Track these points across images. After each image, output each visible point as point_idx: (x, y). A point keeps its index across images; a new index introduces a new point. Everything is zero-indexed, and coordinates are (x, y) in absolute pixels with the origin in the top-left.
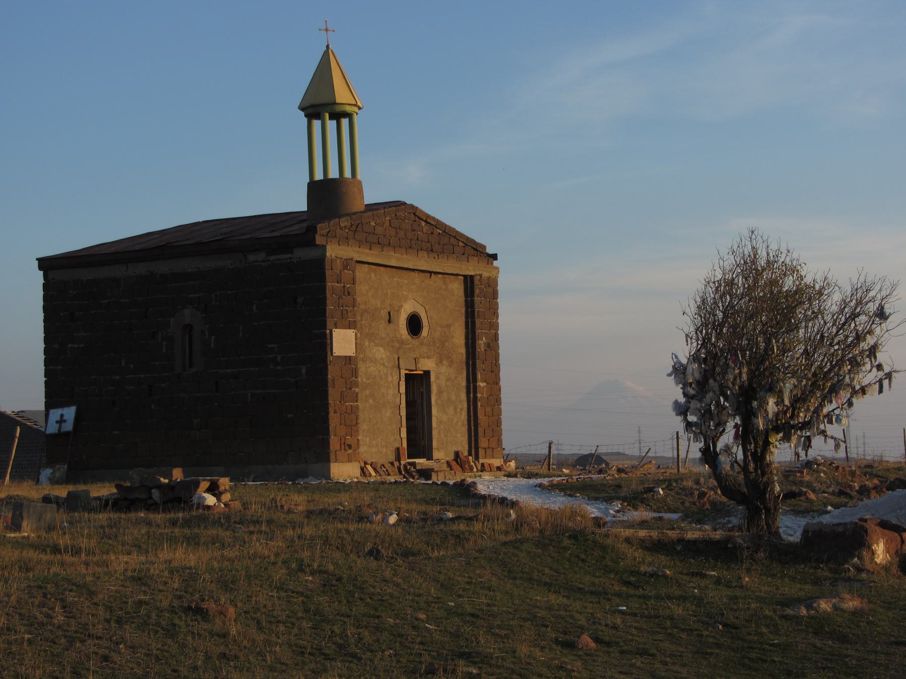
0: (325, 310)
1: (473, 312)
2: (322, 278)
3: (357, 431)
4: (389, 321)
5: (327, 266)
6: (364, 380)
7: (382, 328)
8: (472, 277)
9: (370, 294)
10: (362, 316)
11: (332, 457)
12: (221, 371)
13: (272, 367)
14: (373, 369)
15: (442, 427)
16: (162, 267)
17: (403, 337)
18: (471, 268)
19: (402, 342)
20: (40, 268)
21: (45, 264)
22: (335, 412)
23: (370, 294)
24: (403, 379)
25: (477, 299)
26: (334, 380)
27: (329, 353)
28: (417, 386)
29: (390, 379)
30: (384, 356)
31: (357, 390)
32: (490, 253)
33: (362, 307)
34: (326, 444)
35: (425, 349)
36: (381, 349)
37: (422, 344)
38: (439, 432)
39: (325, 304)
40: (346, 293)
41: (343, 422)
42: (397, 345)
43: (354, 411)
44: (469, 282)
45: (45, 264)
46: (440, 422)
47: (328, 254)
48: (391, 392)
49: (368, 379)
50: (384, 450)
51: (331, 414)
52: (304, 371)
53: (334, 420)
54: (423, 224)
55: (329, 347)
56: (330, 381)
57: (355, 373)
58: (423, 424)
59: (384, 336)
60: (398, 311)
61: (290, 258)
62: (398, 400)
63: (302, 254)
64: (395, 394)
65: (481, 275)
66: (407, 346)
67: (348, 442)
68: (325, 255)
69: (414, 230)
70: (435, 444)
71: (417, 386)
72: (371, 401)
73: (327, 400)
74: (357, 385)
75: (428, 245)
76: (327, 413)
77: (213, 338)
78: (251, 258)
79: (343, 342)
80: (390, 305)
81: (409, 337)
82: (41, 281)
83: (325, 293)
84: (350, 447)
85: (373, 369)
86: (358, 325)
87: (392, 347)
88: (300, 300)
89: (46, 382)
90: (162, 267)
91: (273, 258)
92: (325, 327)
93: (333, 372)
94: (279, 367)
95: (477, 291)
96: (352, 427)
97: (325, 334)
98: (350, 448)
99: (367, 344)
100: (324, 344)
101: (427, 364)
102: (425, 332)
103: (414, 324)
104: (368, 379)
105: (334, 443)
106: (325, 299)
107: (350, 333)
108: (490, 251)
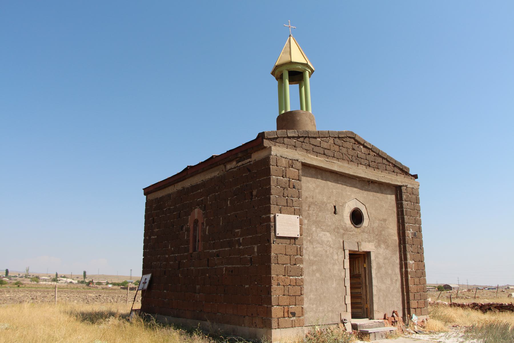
0: (269, 199)
1: (402, 211)
2: (267, 172)
3: (302, 300)
4: (335, 213)
5: (272, 162)
6: (312, 258)
7: (329, 218)
8: (400, 187)
9: (317, 191)
10: (309, 207)
11: (274, 324)
12: (211, 251)
13: (237, 247)
14: (319, 249)
15: (381, 293)
16: (187, 183)
17: (347, 226)
18: (398, 180)
19: (346, 230)
20: (145, 194)
21: (144, 189)
22: (278, 284)
23: (317, 191)
24: (347, 257)
25: (404, 203)
26: (277, 257)
27: (272, 234)
28: (359, 261)
29: (336, 257)
30: (330, 239)
31: (301, 266)
32: (412, 174)
33: (310, 200)
34: (269, 312)
35: (366, 236)
36: (328, 234)
37: (363, 232)
38: (379, 298)
39: (270, 193)
40: (291, 186)
41: (286, 293)
42: (342, 231)
43: (299, 285)
44: (398, 190)
45: (144, 189)
46: (380, 290)
47: (273, 153)
48: (336, 267)
49: (315, 257)
50: (330, 314)
51: (274, 286)
52: (256, 250)
53: (277, 292)
54: (362, 147)
55: (272, 229)
56: (273, 259)
57: (299, 252)
58: (366, 292)
59: (330, 224)
60: (343, 206)
61: (250, 162)
62: (343, 274)
63: (257, 156)
64: (342, 269)
65: (406, 186)
66: (351, 233)
67: (291, 310)
68: (271, 155)
69: (354, 149)
70: (375, 307)
71: (359, 261)
72: (318, 275)
73: (270, 273)
74: (301, 262)
75: (366, 162)
76: (270, 286)
77: (207, 228)
78: (229, 167)
79: (286, 225)
80: (336, 201)
81: (352, 226)
82: (145, 201)
83: (270, 184)
84: (294, 314)
85: (319, 249)
86: (305, 214)
87: (338, 233)
88: (254, 193)
89: (144, 259)
90: (187, 183)
91: (240, 164)
92: (269, 212)
93: (276, 248)
94: (241, 247)
95: (404, 197)
96: (297, 297)
97: (269, 218)
98: (294, 316)
99: (314, 229)
100: (267, 226)
101: (365, 247)
102: (366, 223)
103: (357, 217)
104: (315, 257)
105: (276, 311)
106: (270, 189)
107: (295, 219)
108: (412, 172)
